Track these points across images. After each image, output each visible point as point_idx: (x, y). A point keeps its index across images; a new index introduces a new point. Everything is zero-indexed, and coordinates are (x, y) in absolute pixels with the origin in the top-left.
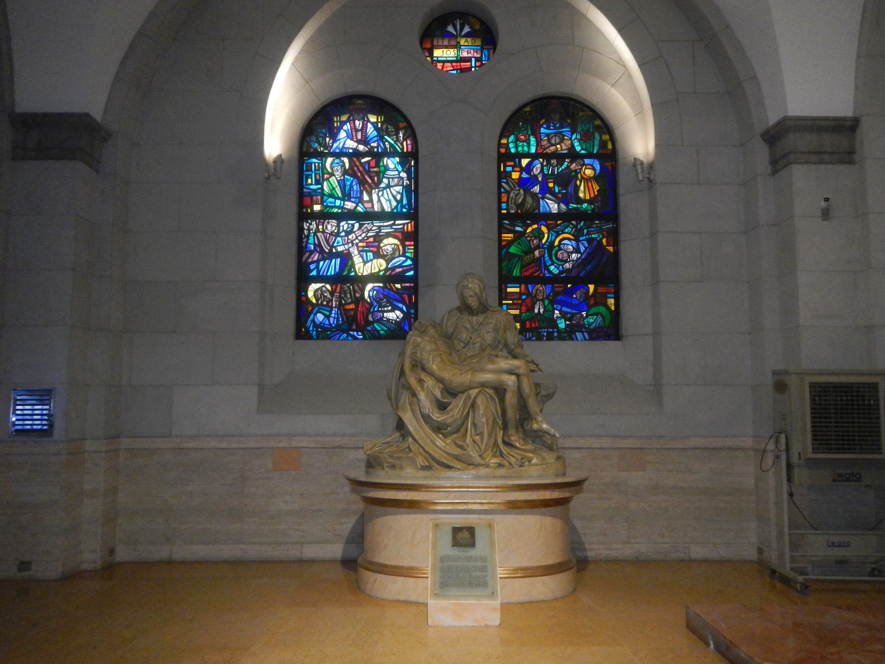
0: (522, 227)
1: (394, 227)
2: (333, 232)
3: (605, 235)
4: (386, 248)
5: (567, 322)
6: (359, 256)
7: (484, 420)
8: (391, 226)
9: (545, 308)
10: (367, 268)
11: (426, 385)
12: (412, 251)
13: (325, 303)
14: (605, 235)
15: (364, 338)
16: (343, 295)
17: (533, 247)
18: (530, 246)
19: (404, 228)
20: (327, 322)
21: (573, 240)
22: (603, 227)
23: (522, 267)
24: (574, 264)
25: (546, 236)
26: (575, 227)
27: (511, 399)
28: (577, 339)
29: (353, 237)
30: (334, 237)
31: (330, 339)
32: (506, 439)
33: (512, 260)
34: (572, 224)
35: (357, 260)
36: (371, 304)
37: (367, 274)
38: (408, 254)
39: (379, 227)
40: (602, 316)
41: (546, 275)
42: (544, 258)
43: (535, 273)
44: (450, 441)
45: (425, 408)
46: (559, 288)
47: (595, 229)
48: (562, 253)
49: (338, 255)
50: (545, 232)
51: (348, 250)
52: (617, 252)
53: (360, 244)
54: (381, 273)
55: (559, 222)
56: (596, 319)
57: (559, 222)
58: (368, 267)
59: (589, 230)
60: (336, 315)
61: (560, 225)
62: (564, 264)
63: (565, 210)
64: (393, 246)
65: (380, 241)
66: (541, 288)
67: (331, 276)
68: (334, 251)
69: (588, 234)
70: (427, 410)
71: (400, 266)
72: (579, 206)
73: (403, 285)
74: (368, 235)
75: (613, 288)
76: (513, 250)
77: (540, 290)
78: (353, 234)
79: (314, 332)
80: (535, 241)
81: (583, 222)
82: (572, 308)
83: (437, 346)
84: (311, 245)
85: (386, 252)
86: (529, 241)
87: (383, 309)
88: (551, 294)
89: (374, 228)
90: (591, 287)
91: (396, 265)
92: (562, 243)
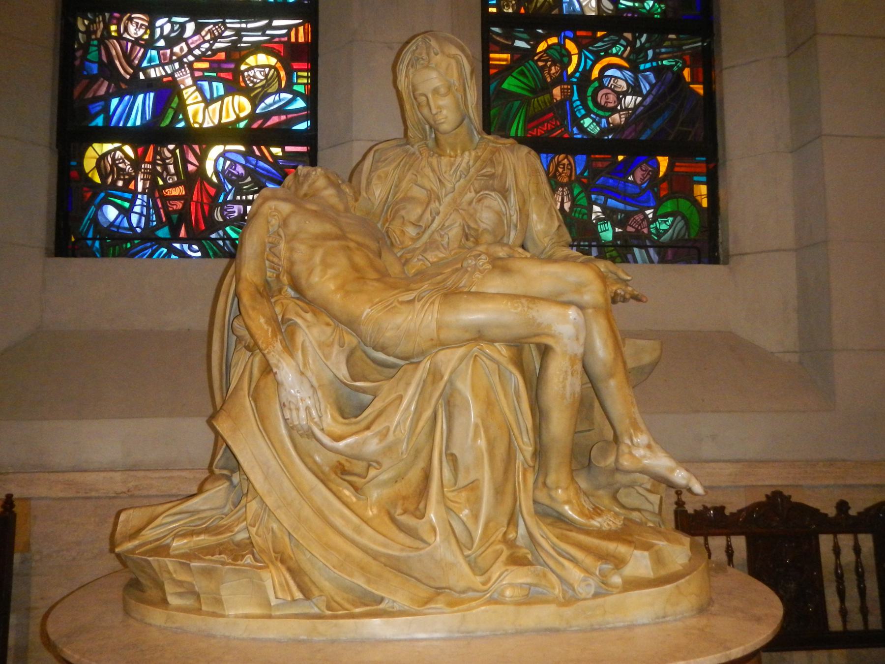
0: (527, 42)
1: (268, 32)
2: (140, 38)
3: (688, 63)
4: (251, 73)
5: (617, 230)
6: (194, 88)
7: (482, 443)
8: (262, 29)
9: (573, 200)
10: (211, 115)
11: (300, 338)
12: (305, 81)
13: (120, 183)
14: (688, 63)
15: (205, 255)
16: (159, 168)
17: (549, 80)
18: (545, 79)
19: (288, 35)
20: (126, 225)
21: (626, 68)
22: (684, 47)
23: (529, 120)
24: (630, 117)
25: (575, 59)
26: (631, 43)
27: (565, 379)
28: (636, 261)
29: (182, 49)
30: (142, 50)
31: (133, 255)
32: (542, 497)
33: (509, 105)
34: (626, 39)
35: (191, 96)
36: (220, 188)
37: (211, 125)
38: (296, 88)
39: (238, 32)
40: (684, 217)
41: (575, 136)
42: (572, 103)
43: (553, 130)
44: (375, 511)
45: (298, 409)
46: (601, 161)
47: (670, 50)
48: (606, 94)
49: (150, 85)
50: (572, 53)
51: (172, 75)
52: (710, 93)
53: (197, 65)
54: (242, 125)
55: (599, 34)
56: (673, 222)
57: (599, 34)
58: (214, 110)
59: (657, 50)
60: (145, 209)
61: (601, 39)
62: (610, 116)
63: (610, 12)
64: (267, 70)
65: (242, 59)
66: (566, 161)
67: (134, 128)
68: (142, 76)
69: (655, 58)
70: (303, 415)
71: (280, 111)
72: (637, 5)
73: (288, 149)
74: (214, 48)
75: (704, 165)
76: (510, 84)
77: (564, 165)
78: (183, 45)
79: (97, 244)
80: (553, 68)
81: (645, 36)
82: (625, 199)
83: (341, 229)
84: (91, 64)
85: (252, 82)
86: (542, 69)
87: (244, 197)
88: (586, 174)
89: (227, 33)
90: (663, 162)
91: (272, 108)
92: (607, 73)
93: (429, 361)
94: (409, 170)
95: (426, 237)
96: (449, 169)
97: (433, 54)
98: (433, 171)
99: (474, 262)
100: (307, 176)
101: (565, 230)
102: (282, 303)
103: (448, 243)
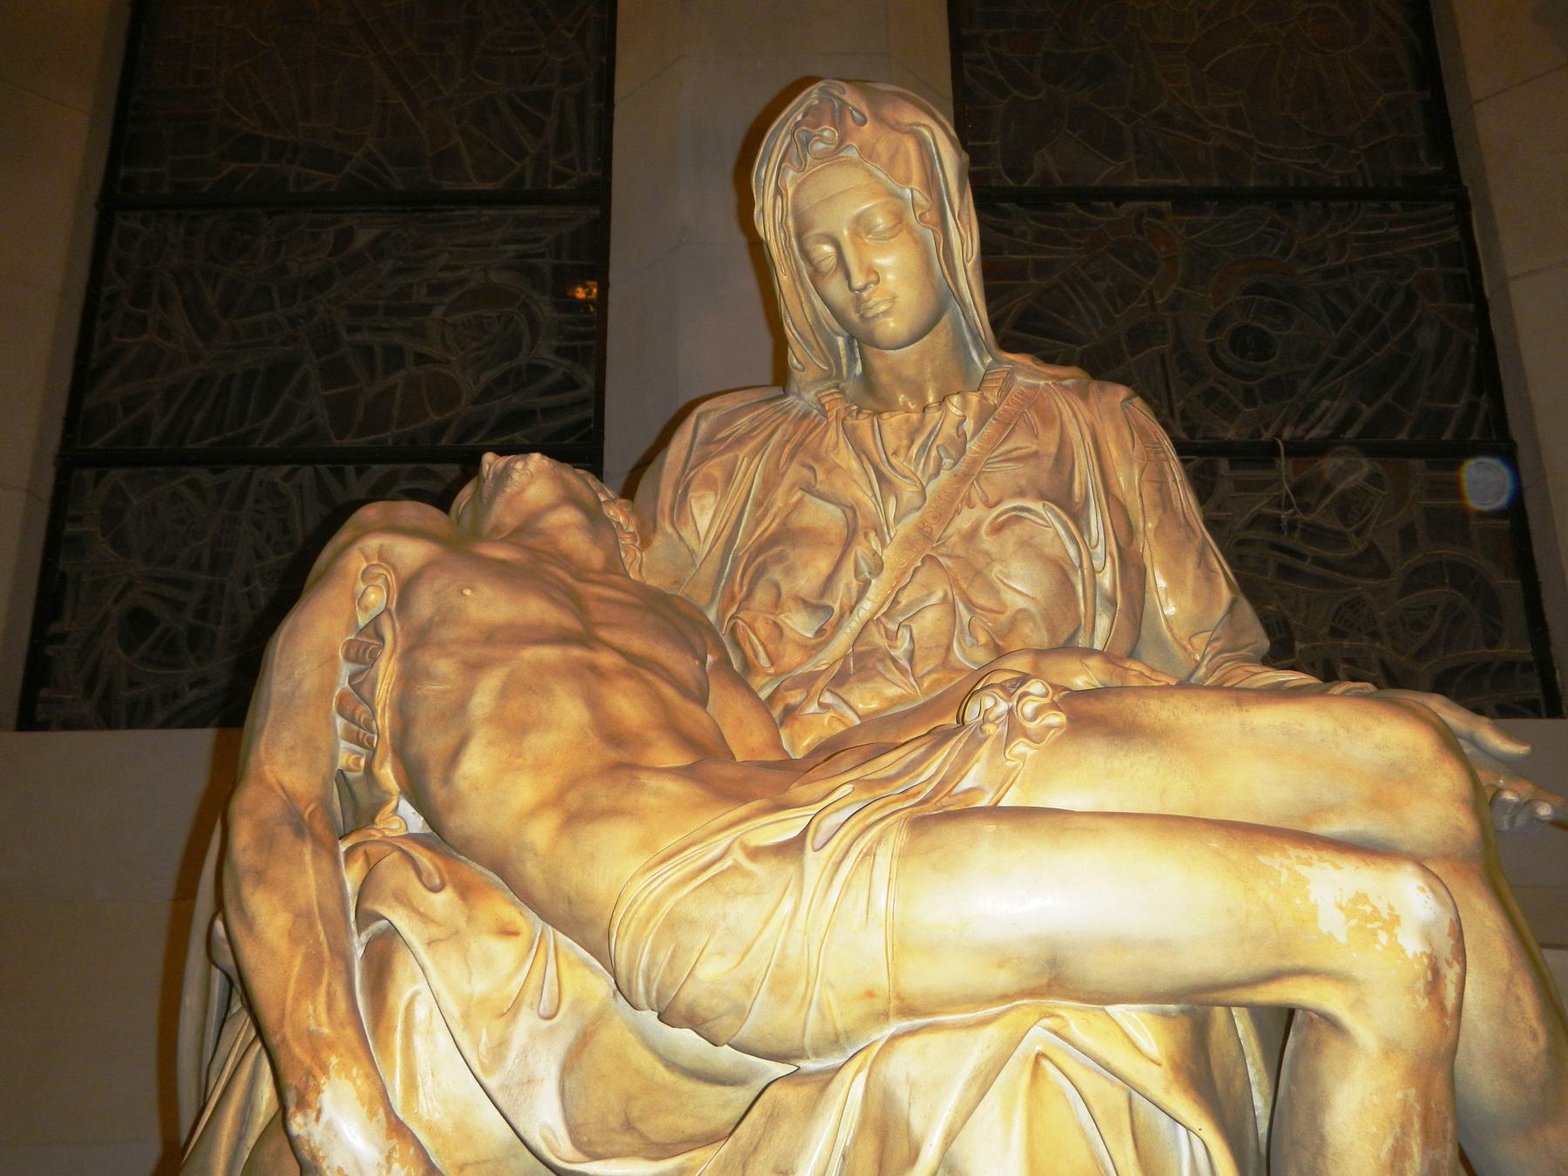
93: (862, 1077)
94: (792, 457)
95: (842, 642)
96: (905, 442)
97: (850, 122)
98: (860, 451)
99: (1003, 707)
100: (503, 476)
101: (1246, 609)
102: (366, 853)
103: (911, 657)
